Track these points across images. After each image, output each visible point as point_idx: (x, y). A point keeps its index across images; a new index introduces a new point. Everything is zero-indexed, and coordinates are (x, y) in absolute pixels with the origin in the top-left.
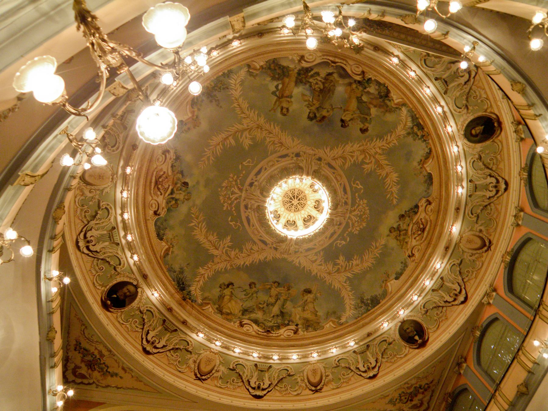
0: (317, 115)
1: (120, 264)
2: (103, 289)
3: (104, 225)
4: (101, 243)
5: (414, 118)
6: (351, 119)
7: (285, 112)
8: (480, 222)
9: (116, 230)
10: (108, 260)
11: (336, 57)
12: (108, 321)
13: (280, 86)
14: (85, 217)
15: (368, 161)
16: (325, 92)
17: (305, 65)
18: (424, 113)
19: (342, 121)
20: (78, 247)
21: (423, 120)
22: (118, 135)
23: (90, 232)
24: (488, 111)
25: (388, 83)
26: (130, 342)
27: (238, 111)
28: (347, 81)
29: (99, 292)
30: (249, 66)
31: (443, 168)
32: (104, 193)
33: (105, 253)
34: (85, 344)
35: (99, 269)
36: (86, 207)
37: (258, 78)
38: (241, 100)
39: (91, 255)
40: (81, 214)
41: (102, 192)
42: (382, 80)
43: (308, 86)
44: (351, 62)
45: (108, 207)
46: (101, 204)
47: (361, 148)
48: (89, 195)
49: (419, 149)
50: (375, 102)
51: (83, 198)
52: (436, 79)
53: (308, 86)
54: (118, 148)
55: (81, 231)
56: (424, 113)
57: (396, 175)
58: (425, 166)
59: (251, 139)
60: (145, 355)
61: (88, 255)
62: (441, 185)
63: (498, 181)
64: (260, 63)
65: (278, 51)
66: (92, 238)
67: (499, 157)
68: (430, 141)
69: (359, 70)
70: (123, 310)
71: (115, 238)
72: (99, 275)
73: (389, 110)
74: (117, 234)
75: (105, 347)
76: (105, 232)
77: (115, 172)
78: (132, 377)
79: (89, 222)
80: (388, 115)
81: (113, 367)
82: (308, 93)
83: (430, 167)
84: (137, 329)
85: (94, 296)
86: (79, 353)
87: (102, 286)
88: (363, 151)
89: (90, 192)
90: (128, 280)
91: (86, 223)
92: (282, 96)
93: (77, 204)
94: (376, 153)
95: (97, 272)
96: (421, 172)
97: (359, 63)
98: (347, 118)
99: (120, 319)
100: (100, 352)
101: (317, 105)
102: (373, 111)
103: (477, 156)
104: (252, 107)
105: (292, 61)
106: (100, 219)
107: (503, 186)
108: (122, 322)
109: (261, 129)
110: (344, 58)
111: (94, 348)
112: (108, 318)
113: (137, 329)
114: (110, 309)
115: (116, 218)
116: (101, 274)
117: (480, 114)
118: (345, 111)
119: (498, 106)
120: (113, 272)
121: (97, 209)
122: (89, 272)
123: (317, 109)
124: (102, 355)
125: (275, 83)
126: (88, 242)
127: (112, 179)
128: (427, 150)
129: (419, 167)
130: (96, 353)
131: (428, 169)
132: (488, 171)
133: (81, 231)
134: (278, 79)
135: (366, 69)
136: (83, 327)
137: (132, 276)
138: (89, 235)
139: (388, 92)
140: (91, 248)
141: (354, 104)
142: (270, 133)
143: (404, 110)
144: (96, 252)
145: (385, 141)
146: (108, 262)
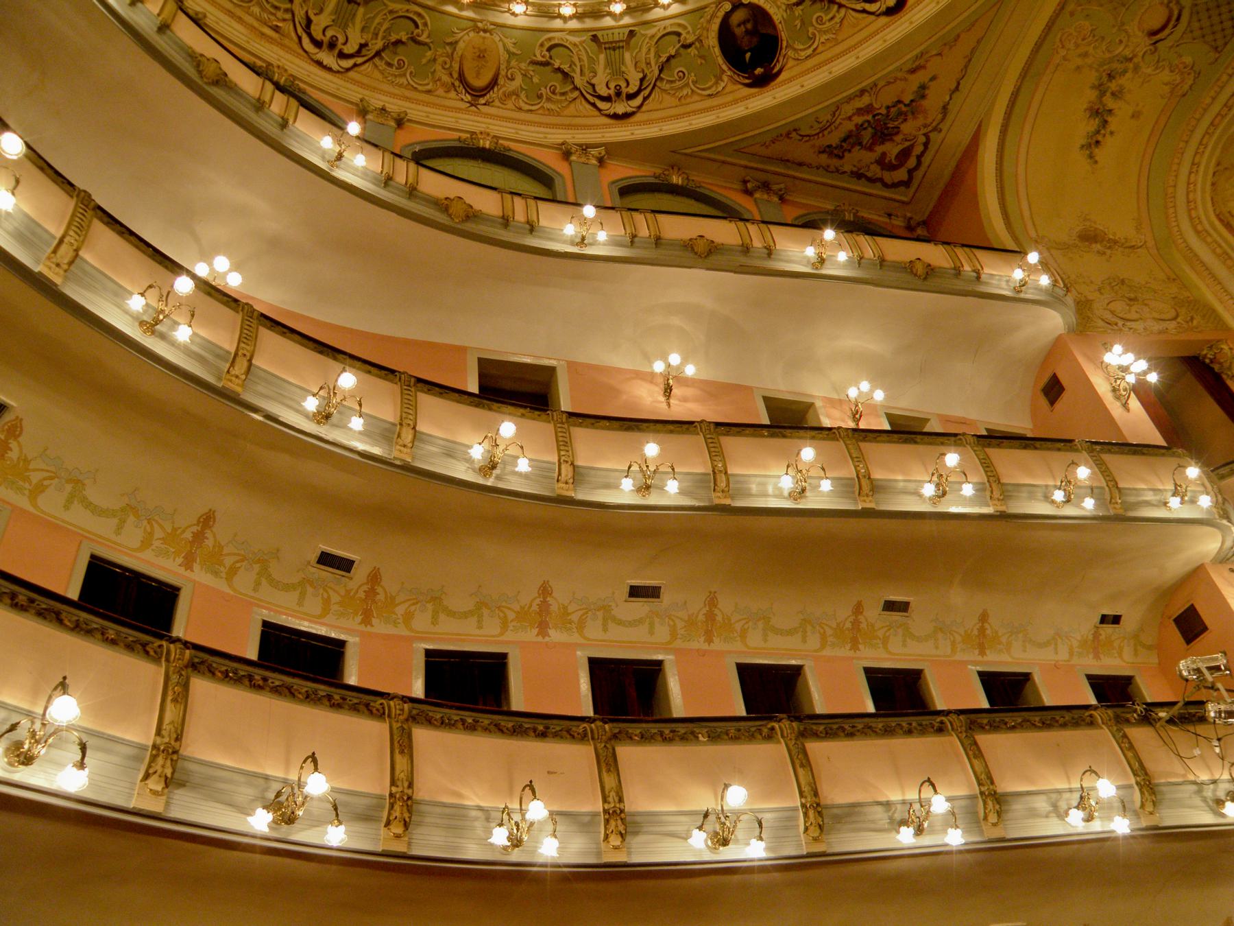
1: (679, 34)
2: (725, 78)
3: (585, 58)
4: (623, 69)
9: (599, 34)
10: (663, 59)
12: (799, 82)
14: (563, 94)
20: (626, 116)
22: (391, 12)
23: (597, 89)
26: (860, 43)
29: (731, 87)
32: (514, 50)
33: (648, 64)
34: (834, 139)
35: (681, 79)
36: (543, 91)
39: (646, 92)
40: (558, 101)
41: (514, 54)
45: (547, 45)
46: (540, 59)
48: (518, 81)
51: (523, 95)
54: (419, 15)
55: (594, 105)
60: (901, 14)
61: (645, 99)
66: (612, 85)
70: (784, 44)
71: (616, 38)
72: (695, 83)
74: (610, 32)
75: (849, 99)
76: (602, 57)
77: (471, 24)
78: (940, 54)
79: (576, 88)
81: (902, 92)
84: (837, 20)
85: (736, 101)
86: (850, 151)
87: (719, 79)
89: (513, 79)
90: (718, 21)
91: (576, 94)
93: (533, 108)
95: (687, 85)
99: (803, 54)
100: (860, 111)
106: (572, 64)
108: (809, 51)
111: (846, 123)
112: (790, 80)
113: (837, 20)
114: (776, 70)
115: (573, 32)
116: (693, 77)
120: (692, 51)
121: (549, 68)
122: (683, 101)
124: (868, 109)
126: (618, 94)
127: (485, 31)
130: (859, 120)
133: (594, 105)
136: (794, 135)
137: (710, 11)
138: (603, 92)
140: (632, 89)
144: (642, 80)
146: (668, 59)
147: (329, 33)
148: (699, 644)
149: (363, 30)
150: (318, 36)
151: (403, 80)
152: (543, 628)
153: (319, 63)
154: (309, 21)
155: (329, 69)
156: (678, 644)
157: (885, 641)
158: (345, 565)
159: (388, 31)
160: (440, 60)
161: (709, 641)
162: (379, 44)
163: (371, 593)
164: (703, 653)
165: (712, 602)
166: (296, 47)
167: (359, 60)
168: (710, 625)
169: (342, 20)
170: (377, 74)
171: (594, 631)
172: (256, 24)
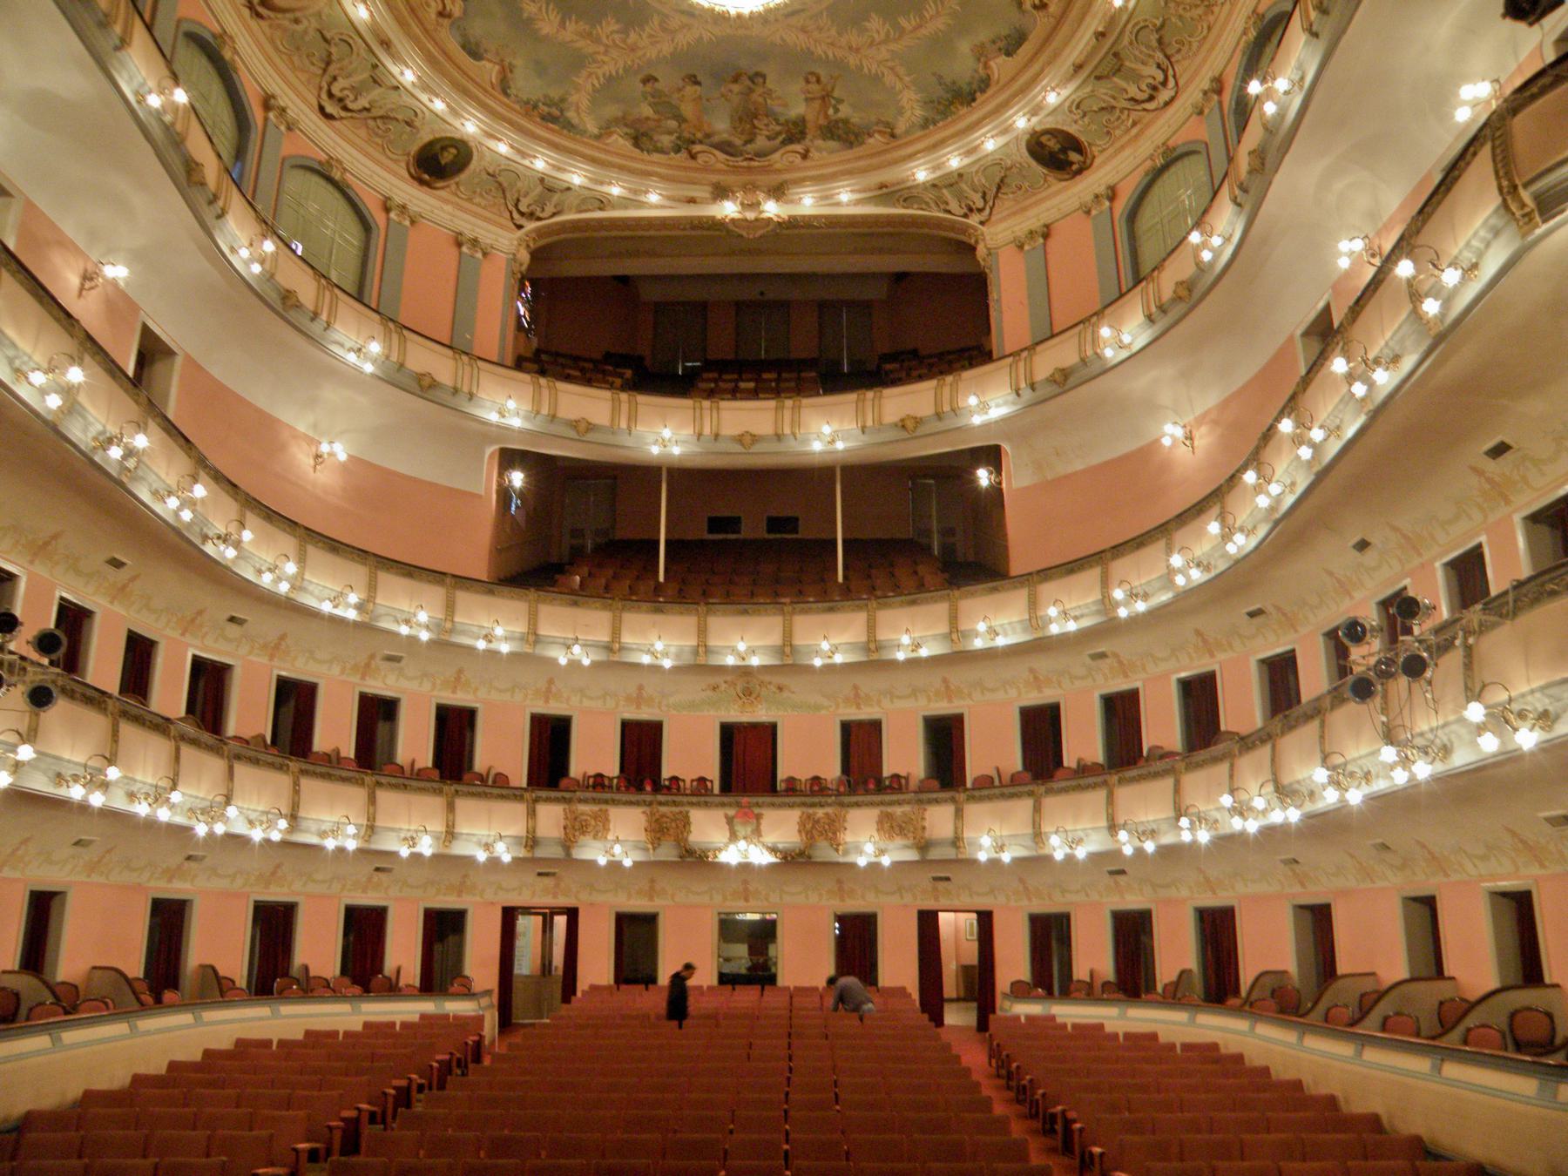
0: (748, 83)
5: (569, 126)
6: (680, 90)
7: (812, 77)
8: (312, 33)
11: (749, 169)
13: (831, 111)
15: (616, 36)
16: (748, 118)
17: (799, 148)
18: (556, 139)
19: (697, 83)
21: (552, 130)
22: (1131, 43)
24: (453, 187)
25: (645, 156)
27: (901, 71)
28: (716, 139)
30: (893, 136)
31: (463, 81)
37: (873, 118)
38: (899, 86)
42: (656, 157)
43: (782, 120)
44: (720, 166)
47: (640, 53)
49: (527, 84)
50: (651, 124)
52: (569, 189)
53: (782, 120)
56: (556, 139)
57: (544, 32)
58: (497, 67)
59: (867, 30)
62: (444, 53)
63: (345, 109)
64: (876, 141)
65: (849, 161)
67: (379, 141)
68: (517, 107)
69: (701, 159)
73: (622, 121)
80: (620, 114)
82: (779, 110)
83: (489, 70)
88: (633, 49)
92: (823, 98)
94: (606, 53)
96: (497, 54)
97: (706, 169)
98: (691, 90)
101: (755, 97)
102: (647, 111)
103: (417, 123)
104: (877, 79)
105: (819, 150)
107: (329, 109)
109: (850, 48)
110: (736, 170)
117: (463, 177)
118: (700, 98)
119: (446, 201)
123: (751, 91)
125: (841, 115)
128: (512, 91)
129: (507, 61)
131: (489, 65)
132: (375, 112)
134: (837, 122)
135: (692, 164)
139: (637, 141)
141: (688, 110)
142: (832, 44)
143: (593, 128)
145: (600, 72)
147: (1144, 87)
149: (1144, 63)
150: (1146, 96)
151: (1195, 45)
153: (1167, 104)
154: (1132, 99)
155: (1172, 99)
159: (1147, 47)
160: (1181, 11)
161: (1420, 555)
162: (1159, 56)
164: (1423, 566)
165: (1395, 529)
166: (1151, 115)
167: (1171, 72)
169: (1136, 77)
170: (1186, 63)
172: (1127, 138)
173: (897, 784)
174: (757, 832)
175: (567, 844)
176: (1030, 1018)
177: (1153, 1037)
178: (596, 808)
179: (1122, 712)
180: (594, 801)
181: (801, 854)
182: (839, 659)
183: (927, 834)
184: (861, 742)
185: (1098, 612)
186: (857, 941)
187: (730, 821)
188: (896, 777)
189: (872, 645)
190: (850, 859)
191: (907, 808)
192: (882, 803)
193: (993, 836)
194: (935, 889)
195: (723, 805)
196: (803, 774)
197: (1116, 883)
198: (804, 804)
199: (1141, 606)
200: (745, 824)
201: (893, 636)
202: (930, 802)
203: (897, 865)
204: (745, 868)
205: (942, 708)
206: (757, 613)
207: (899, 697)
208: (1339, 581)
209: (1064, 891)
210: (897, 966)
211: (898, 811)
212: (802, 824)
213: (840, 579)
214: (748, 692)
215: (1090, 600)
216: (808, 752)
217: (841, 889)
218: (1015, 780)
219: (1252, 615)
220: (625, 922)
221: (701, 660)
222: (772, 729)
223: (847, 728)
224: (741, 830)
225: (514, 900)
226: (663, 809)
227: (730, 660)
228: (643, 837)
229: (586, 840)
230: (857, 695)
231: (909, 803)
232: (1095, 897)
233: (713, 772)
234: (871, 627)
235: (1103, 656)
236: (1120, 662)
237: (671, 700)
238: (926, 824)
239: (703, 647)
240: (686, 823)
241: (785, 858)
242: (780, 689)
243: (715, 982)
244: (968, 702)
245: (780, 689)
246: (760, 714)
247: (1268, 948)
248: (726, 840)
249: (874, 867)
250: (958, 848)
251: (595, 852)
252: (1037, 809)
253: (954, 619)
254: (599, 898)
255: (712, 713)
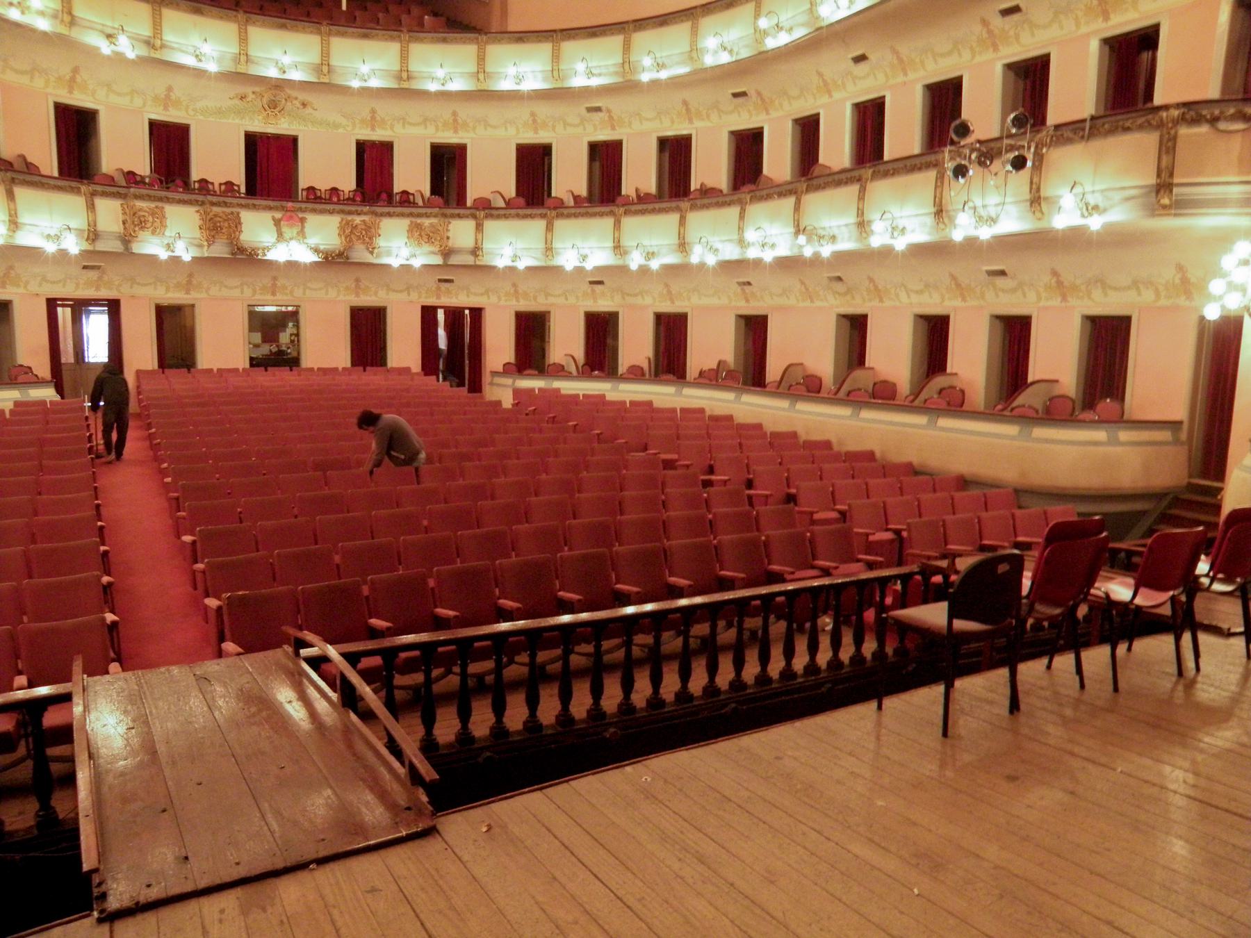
148: (901, 78)
152: (830, 93)
156: (892, 82)
157: (1017, 37)
158: (744, 94)
161: (906, 74)
163: (763, 100)
168: (903, 65)
171: (850, 87)
173: (406, 199)
174: (302, 234)
175: (127, 239)
176: (540, 389)
177: (650, 403)
178: (153, 205)
179: (606, 158)
180: (150, 198)
181: (341, 254)
182: (375, 83)
183: (450, 243)
184: (374, 161)
185: (616, 73)
186: (368, 330)
187: (277, 223)
188: (405, 193)
189: (404, 74)
190: (385, 260)
191: (434, 221)
192: (411, 215)
193: (512, 246)
194: (439, 289)
195: (270, 208)
196: (323, 185)
197: (593, 291)
198: (342, 212)
199: (664, 75)
200: (291, 226)
201: (424, 69)
202: (453, 216)
203: (425, 266)
204: (292, 265)
205: (449, 137)
206: (294, 29)
207: (411, 124)
208: (824, 81)
209: (547, 295)
210: (403, 348)
211: (426, 222)
212: (342, 229)
213: (344, 7)
214: (273, 105)
215: (611, 62)
216: (326, 163)
217: (357, 287)
218: (509, 204)
219: (735, 95)
220: (163, 313)
221: (242, 69)
222: (294, 140)
223: (362, 148)
224: (288, 232)
225: (57, 292)
226: (216, 209)
227: (273, 73)
228: (197, 234)
229: (145, 235)
230: (373, 118)
231: (435, 216)
232: (572, 300)
233: (239, 178)
234: (404, 57)
235: (598, 109)
236: (611, 117)
237: (200, 105)
238: (450, 234)
239: (244, 55)
240: (238, 223)
241: (326, 258)
242: (304, 105)
243: (247, 366)
244: (472, 135)
245: (304, 105)
246: (281, 126)
247: (712, 343)
248: (274, 240)
249: (406, 268)
250: (477, 256)
251: (151, 246)
252: (549, 228)
253: (481, 59)
254: (140, 291)
255: (237, 121)
